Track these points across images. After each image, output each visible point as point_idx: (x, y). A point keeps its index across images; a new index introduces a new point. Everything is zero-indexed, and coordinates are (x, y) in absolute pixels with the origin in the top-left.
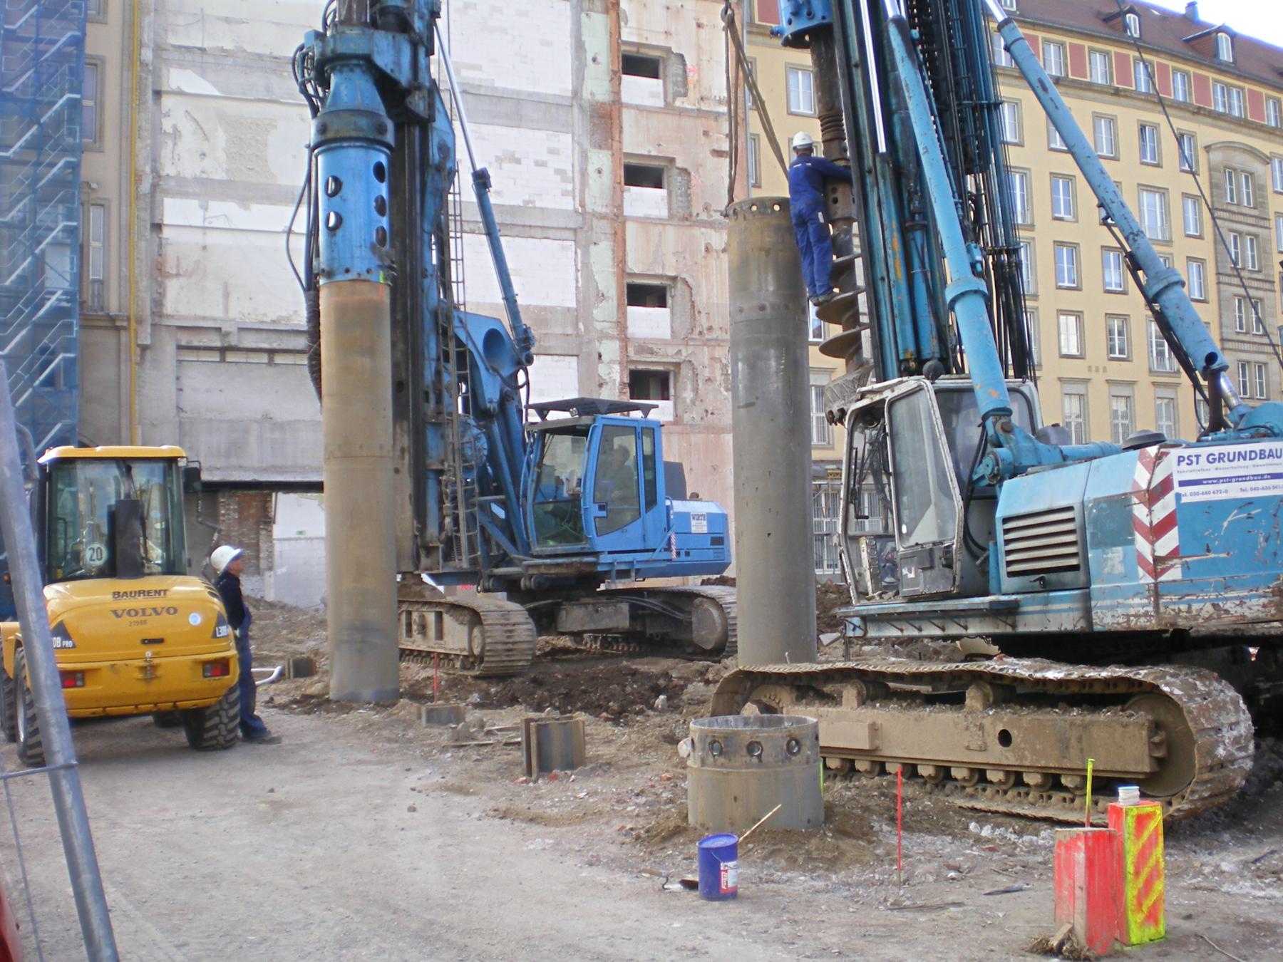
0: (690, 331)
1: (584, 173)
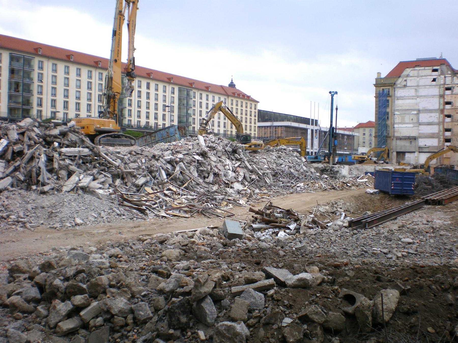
0: (453, 135)
1: (440, 117)
